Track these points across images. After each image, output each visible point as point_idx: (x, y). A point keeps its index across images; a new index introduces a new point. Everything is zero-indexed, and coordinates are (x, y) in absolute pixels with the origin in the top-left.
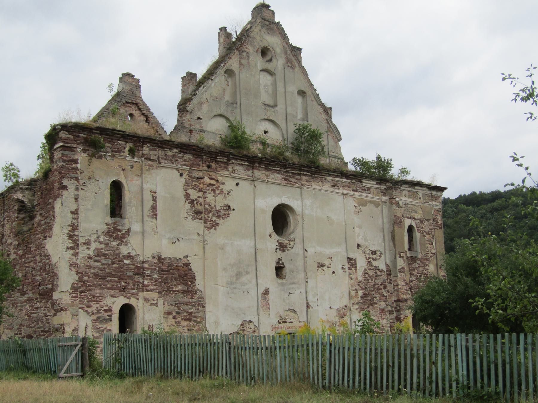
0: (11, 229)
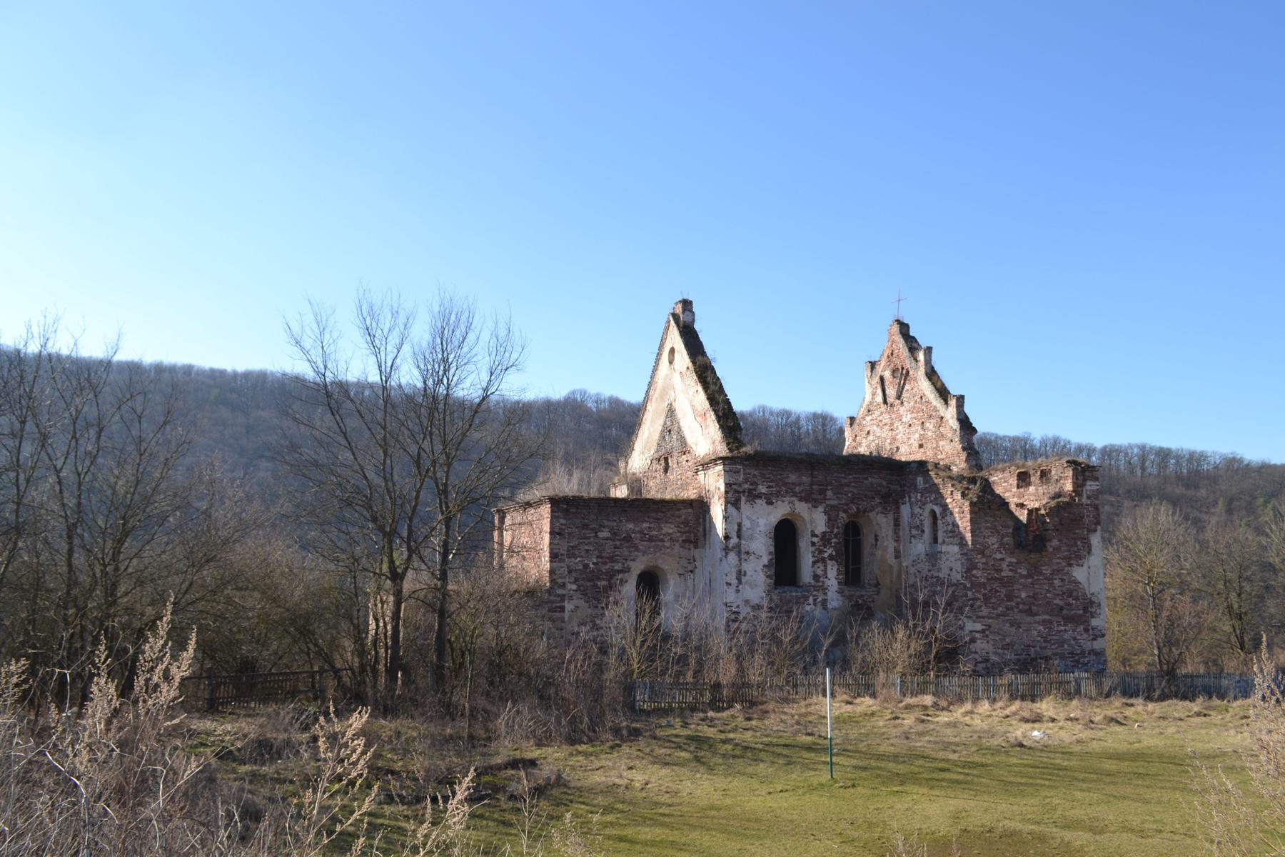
0: (1002, 544)
